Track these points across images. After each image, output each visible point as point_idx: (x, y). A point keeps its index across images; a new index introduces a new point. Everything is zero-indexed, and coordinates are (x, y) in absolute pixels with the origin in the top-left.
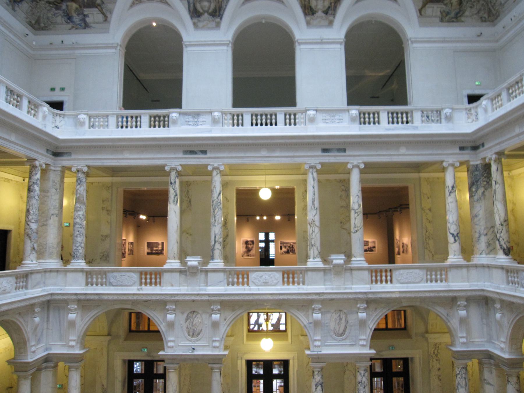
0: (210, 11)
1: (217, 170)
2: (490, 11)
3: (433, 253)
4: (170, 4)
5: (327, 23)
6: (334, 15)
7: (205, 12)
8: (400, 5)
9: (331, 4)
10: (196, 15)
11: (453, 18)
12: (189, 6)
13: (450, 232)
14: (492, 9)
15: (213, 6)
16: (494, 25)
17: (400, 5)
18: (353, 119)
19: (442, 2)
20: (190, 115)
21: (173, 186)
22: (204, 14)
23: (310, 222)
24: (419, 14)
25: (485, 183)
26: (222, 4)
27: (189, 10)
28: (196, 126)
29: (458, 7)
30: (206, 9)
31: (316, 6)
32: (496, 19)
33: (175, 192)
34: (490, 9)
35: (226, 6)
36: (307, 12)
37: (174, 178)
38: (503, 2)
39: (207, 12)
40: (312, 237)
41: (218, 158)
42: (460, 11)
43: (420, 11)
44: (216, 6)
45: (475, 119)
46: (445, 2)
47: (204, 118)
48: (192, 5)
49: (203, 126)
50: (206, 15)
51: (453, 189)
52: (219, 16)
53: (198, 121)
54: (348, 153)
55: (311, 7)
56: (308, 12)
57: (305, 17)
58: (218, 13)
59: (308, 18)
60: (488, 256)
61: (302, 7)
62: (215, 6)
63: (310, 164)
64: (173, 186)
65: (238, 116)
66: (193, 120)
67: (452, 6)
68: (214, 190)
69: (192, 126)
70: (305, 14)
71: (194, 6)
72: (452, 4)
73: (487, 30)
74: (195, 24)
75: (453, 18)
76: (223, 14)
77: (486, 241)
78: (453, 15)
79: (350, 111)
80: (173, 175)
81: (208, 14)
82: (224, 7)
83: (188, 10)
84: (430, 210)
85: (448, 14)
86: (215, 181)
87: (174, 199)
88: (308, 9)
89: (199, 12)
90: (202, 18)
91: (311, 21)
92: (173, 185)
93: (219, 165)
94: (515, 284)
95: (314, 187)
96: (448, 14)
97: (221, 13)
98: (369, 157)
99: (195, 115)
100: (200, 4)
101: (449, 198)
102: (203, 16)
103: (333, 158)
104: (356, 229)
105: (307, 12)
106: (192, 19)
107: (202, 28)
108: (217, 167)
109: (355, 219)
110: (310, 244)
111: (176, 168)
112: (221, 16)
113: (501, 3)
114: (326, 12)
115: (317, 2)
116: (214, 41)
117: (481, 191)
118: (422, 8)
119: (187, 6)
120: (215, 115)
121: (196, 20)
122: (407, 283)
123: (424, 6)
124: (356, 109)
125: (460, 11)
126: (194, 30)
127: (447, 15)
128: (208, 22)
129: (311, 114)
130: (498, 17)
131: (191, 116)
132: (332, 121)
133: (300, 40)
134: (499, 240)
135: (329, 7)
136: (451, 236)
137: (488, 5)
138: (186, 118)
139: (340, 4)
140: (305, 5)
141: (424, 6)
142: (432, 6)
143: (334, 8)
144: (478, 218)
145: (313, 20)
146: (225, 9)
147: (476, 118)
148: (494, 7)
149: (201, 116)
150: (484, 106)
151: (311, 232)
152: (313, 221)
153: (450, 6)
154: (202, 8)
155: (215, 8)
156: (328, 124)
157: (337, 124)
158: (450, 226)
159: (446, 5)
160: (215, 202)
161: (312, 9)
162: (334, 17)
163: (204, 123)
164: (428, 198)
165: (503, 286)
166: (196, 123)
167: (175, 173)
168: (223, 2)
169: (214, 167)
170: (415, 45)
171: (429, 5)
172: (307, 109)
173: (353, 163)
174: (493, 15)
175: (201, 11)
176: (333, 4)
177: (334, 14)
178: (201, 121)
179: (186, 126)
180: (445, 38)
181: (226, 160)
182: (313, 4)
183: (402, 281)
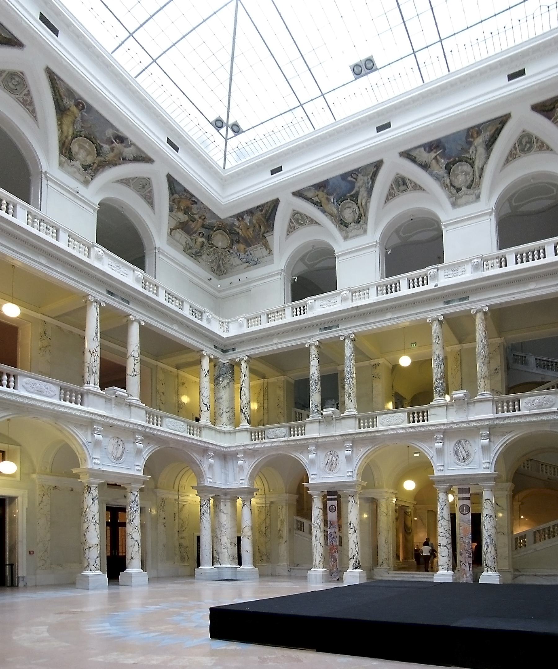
9: (94, 163)
19: (190, 236)
24: (169, 232)
29: (200, 248)
31: (77, 153)
42: (200, 252)
43: (171, 230)
55: (70, 149)
67: (196, 242)
72: (196, 242)
78: (194, 251)
96: (191, 248)
123: (176, 228)
125: (200, 252)
127: (189, 249)
135: (90, 166)
139: (103, 171)
140: (65, 142)
141: (176, 228)
143: (95, 170)
153: (194, 243)
159: (192, 239)
162: (92, 179)
176: (95, 165)
182: (75, 148)
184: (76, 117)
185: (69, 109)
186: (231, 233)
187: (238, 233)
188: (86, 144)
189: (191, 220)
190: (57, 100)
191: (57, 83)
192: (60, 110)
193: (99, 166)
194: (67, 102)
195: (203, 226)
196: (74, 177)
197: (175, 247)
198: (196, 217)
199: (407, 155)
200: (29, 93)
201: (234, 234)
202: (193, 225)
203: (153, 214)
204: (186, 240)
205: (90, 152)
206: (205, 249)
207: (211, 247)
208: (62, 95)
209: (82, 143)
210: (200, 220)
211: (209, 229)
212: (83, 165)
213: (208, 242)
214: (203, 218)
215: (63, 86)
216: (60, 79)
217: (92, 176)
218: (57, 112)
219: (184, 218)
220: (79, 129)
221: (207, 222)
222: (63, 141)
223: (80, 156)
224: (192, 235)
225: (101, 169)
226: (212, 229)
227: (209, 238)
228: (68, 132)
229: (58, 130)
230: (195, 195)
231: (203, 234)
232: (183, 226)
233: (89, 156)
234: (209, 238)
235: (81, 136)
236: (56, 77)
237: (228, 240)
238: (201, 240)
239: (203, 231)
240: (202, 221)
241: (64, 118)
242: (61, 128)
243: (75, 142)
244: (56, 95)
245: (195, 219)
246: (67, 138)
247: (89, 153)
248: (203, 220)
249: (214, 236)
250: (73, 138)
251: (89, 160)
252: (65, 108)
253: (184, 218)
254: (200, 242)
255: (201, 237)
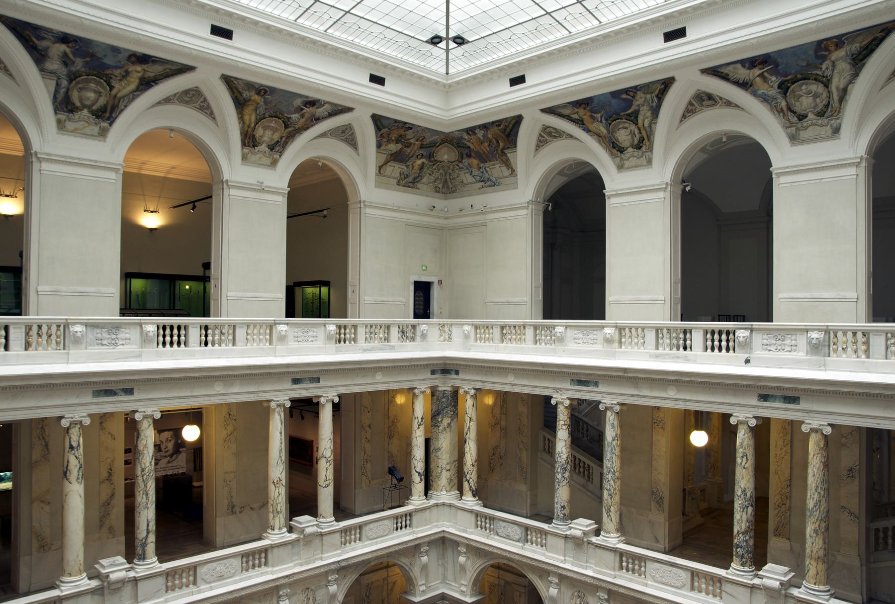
0: (94, 108)
1: (149, 419)
2: (446, 182)
3: (370, 479)
4: (14, 73)
5: (268, 161)
6: (281, 154)
7: (84, 106)
8: (359, 155)
9: (281, 138)
10: (66, 107)
11: (410, 182)
12: (56, 92)
13: (416, 472)
14: (448, 180)
15: (102, 101)
16: (446, 199)
17: (359, 155)
18: (329, 337)
20: (104, 328)
21: (76, 452)
22: (82, 110)
23: (275, 481)
24: (378, 172)
25: (452, 413)
26: (119, 102)
27: (55, 98)
28: (113, 347)
30: (88, 103)
31: (262, 137)
32: (450, 193)
33: (79, 462)
34: (446, 180)
35: (126, 106)
36: (246, 142)
37: (78, 438)
38: (465, 182)
39: (89, 108)
40: (278, 502)
41: (151, 399)
42: (419, 176)
43: (380, 167)
44: (107, 102)
45: (447, 339)
46: (408, 164)
47: (127, 333)
48: (63, 91)
49: (126, 346)
50: (85, 112)
51: (422, 421)
52: (108, 119)
53: (118, 339)
54: (322, 383)
55: (254, 136)
56: (248, 143)
57: (242, 148)
58: (107, 115)
59: (246, 150)
60: (449, 494)
61: (241, 134)
62: (105, 103)
63: (278, 401)
64: (76, 452)
65: (179, 328)
66: (109, 336)
68: (145, 452)
69: (107, 347)
70: (244, 144)
71: (67, 93)
72: (413, 166)
73: (440, 203)
74: (59, 122)
75: (410, 182)
76: (116, 118)
77: (448, 477)
78: (410, 179)
79: (327, 326)
80: (75, 434)
81: (89, 111)
82: (123, 107)
83: (52, 97)
84: (370, 427)
85: (407, 177)
86: (146, 437)
87: (78, 475)
88: (249, 138)
89: (74, 104)
90: (77, 116)
91: (249, 155)
92: (76, 450)
93: (153, 411)
94: (486, 530)
95: (281, 434)
96: (407, 177)
97: (114, 115)
98: (344, 388)
99: (112, 328)
100: (79, 92)
101: (418, 431)
102: (79, 113)
103: (305, 391)
104: (327, 482)
105: (246, 142)
106: (56, 113)
107: (72, 132)
108: (150, 415)
109: (327, 469)
110: (275, 512)
111: (81, 422)
112: (111, 120)
113: (462, 182)
114: (272, 148)
115: (264, 132)
116: (96, 161)
117: (446, 421)
118: (383, 165)
119: (52, 89)
120: (148, 330)
121: (62, 116)
122: (376, 538)
123: (386, 163)
124: (333, 324)
125: (419, 176)
126: (57, 133)
127: (405, 178)
128: (87, 125)
129: (282, 331)
130: (453, 192)
131: (106, 330)
132: (306, 339)
133: (232, 182)
134: (468, 482)
135: (278, 142)
136: (417, 474)
137: (446, 175)
138: (97, 334)
139: (293, 141)
140: (247, 131)
141: (386, 163)
142: (394, 165)
144: (441, 451)
145: (252, 153)
146: (122, 110)
147: (449, 337)
148: (453, 181)
149: (124, 330)
150: (466, 332)
151: (277, 494)
152: (280, 480)
153: (411, 168)
154: (81, 100)
155: (105, 106)
156: (300, 343)
157: (311, 343)
158: (416, 465)
159: (407, 166)
160: (147, 470)
161: (255, 139)
162: (280, 156)
163: (128, 341)
164: (369, 412)
165: (471, 530)
166: (113, 342)
167: (78, 429)
168: (122, 100)
169: (146, 415)
170: (368, 210)
171: (392, 163)
172: (276, 322)
173: (327, 397)
174: (448, 187)
175: (78, 104)
176: (284, 139)
177: (281, 152)
178: (122, 339)
179: (97, 347)
180: (399, 207)
181: (163, 402)
182: (259, 132)
183: (372, 537)
184: (258, 104)
185: (250, 100)
186: (459, 147)
187: (469, 147)
188: (271, 122)
189: (406, 147)
190: (236, 97)
191: (234, 84)
192: (240, 104)
193: (287, 139)
194: (246, 94)
195: (422, 147)
196: (262, 165)
197: (387, 187)
198: (412, 141)
199: (715, 72)
200: (205, 100)
201: (463, 147)
202: (409, 150)
203: (357, 155)
204: (400, 170)
205: (276, 128)
206: (425, 170)
207: (434, 164)
208: (241, 90)
209: (267, 124)
210: (417, 143)
211: (429, 147)
212: (269, 145)
213: (430, 161)
214: (421, 139)
215: (241, 83)
216: (236, 79)
217: (281, 152)
218: (236, 107)
219: (393, 147)
220: (262, 112)
221: (427, 141)
222: (245, 132)
223: (265, 138)
224: (407, 161)
225: (290, 141)
226: (433, 146)
227: (430, 157)
228: (250, 120)
229: (240, 123)
230: (408, 121)
231: (423, 155)
232: (397, 157)
233: (276, 134)
234: (430, 157)
235: (265, 118)
236: (232, 79)
237: (456, 153)
238: (419, 162)
239: (422, 151)
240: (420, 143)
241: (245, 110)
242: (242, 120)
243: (259, 127)
244: (233, 93)
245: (411, 144)
246: (249, 126)
247: (275, 130)
248: (421, 141)
249: (438, 151)
250: (257, 123)
251: (276, 137)
252: (245, 100)
253: (393, 147)
254: (419, 165)
255: (420, 159)
